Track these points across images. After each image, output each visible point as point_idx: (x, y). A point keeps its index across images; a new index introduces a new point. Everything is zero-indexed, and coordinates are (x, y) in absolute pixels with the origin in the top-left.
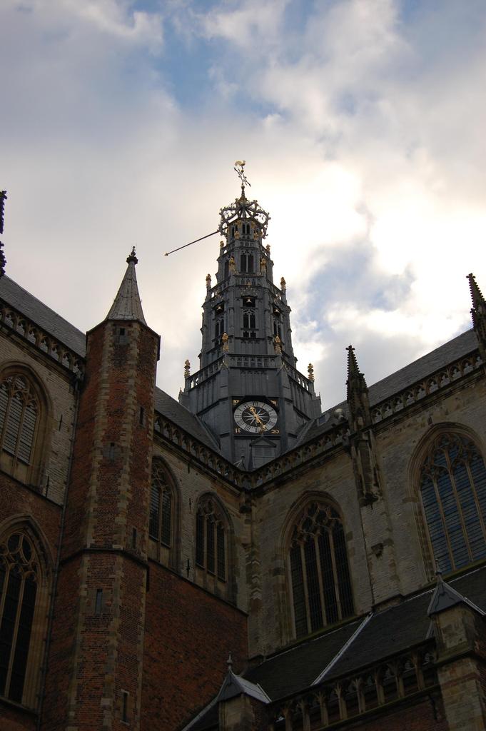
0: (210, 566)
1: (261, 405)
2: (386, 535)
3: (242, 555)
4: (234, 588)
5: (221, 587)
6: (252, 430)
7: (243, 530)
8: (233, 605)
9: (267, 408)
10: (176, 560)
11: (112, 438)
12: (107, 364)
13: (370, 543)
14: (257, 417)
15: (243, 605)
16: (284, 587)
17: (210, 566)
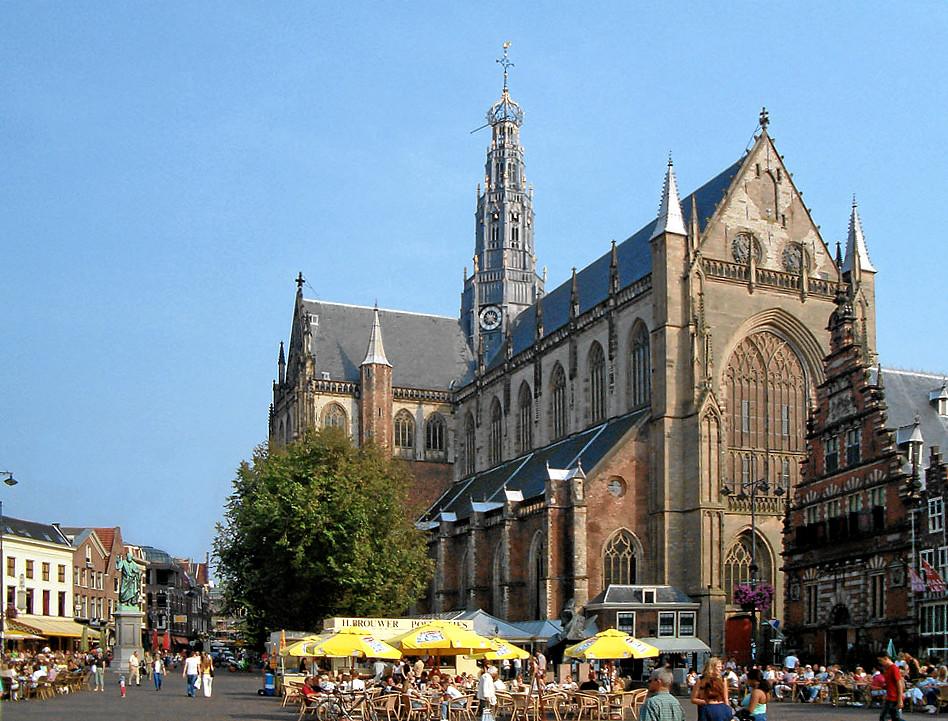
0: (435, 447)
1: (493, 308)
2: (481, 444)
3: (451, 435)
4: (446, 453)
5: (441, 454)
6: (488, 328)
7: (451, 423)
8: (444, 461)
9: (497, 311)
10: (414, 456)
11: (369, 426)
12: (364, 390)
13: (477, 446)
14: (490, 317)
15: (451, 460)
16: (464, 452)
17: (435, 447)
